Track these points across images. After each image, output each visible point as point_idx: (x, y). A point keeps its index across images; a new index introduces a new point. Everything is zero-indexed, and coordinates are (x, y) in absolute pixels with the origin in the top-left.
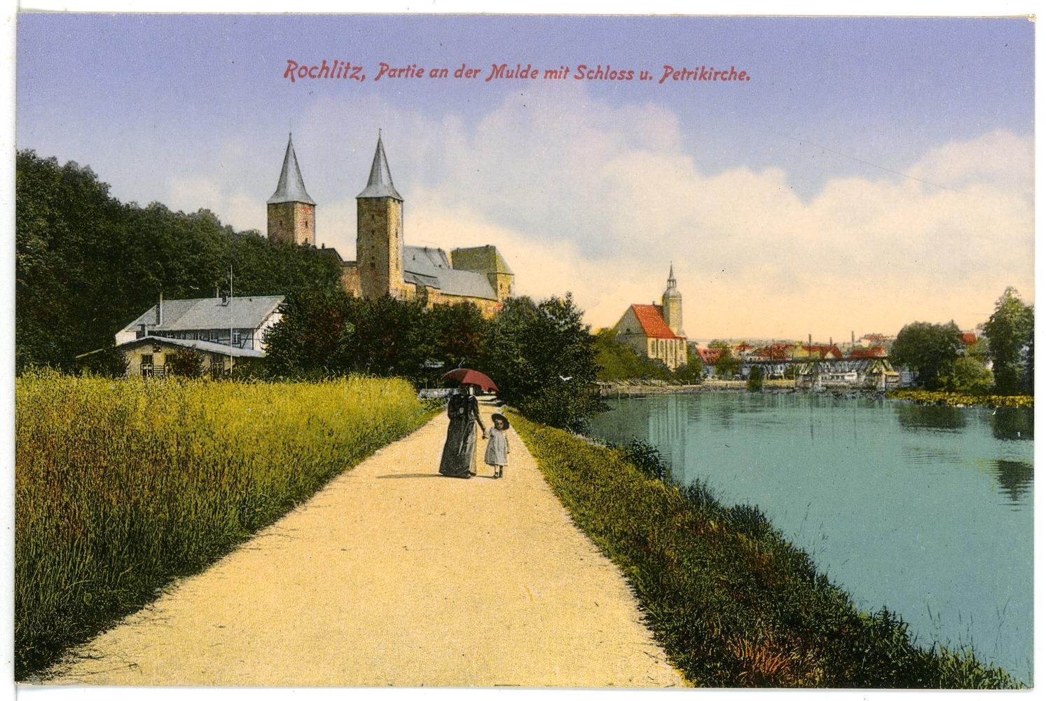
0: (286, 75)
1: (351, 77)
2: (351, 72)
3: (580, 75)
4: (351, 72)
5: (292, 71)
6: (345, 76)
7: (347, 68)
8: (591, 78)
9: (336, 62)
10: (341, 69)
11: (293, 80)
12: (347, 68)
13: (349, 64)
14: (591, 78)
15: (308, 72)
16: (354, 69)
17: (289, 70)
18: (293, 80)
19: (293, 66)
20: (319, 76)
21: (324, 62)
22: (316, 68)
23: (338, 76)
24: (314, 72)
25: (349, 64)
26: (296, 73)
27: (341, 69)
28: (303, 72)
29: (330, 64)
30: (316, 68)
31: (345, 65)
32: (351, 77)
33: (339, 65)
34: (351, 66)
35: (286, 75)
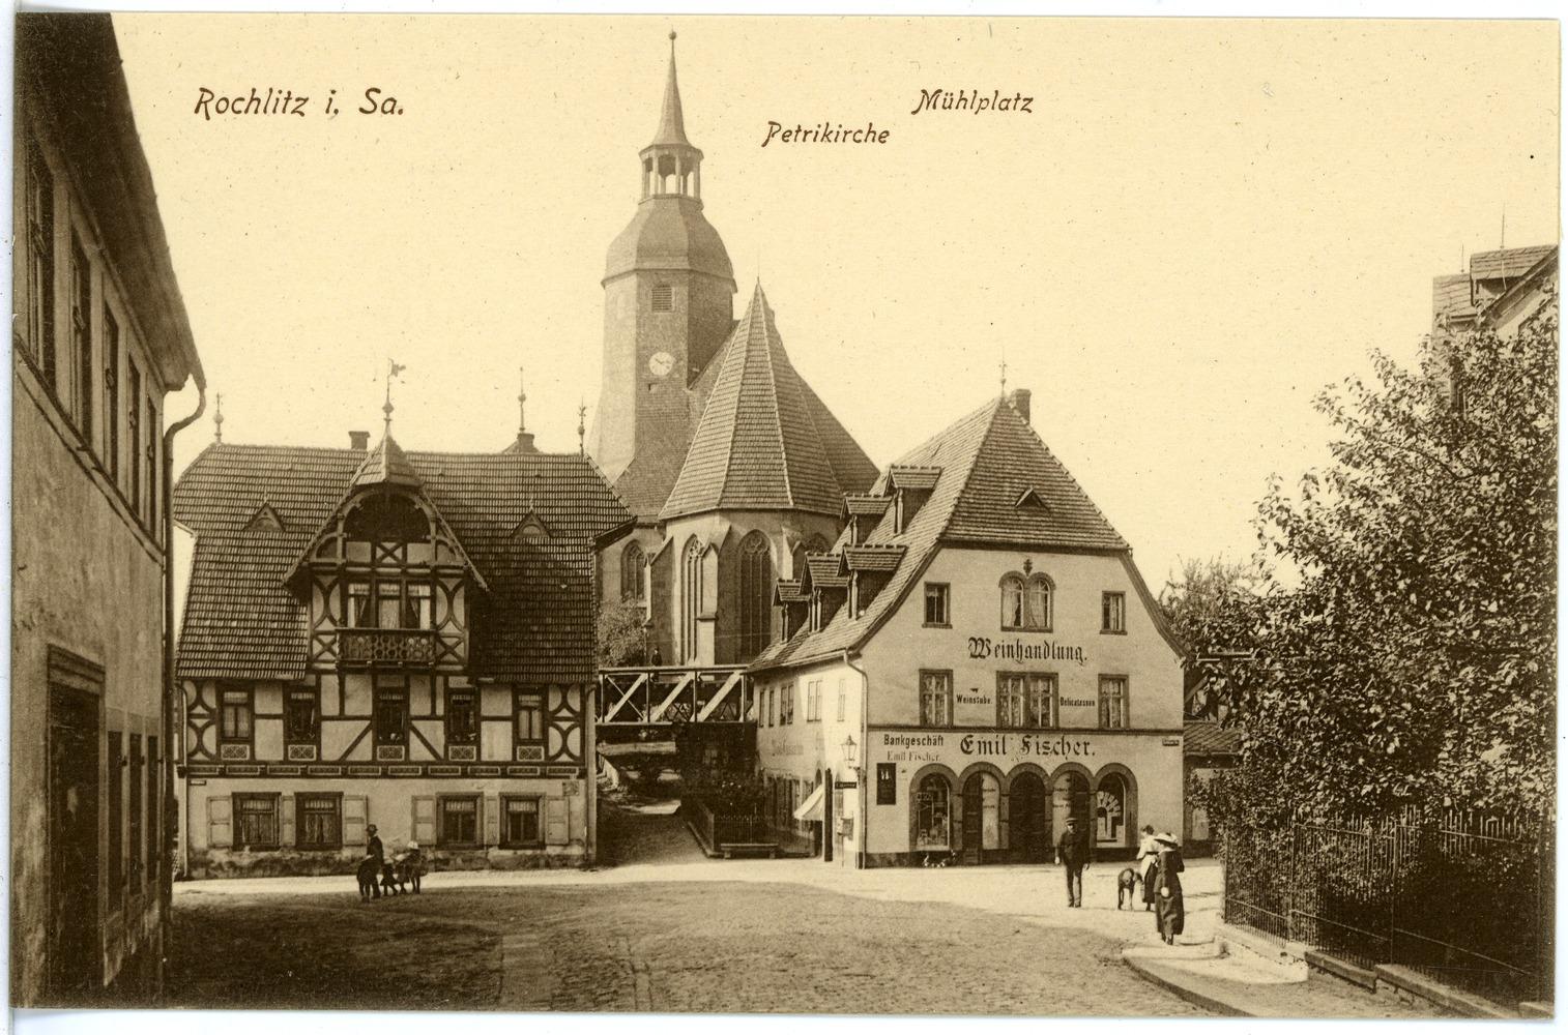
0: (197, 111)
1: (293, 112)
2: (292, 104)
3: (370, 107)
4: (292, 104)
6: (284, 111)
7: (288, 99)
8: (239, 112)
9: (271, 90)
11: (208, 118)
12: (288, 99)
13: (289, 93)
14: (239, 112)
15: (228, 105)
16: (298, 100)
17: (200, 102)
18: (208, 118)
19: (207, 96)
20: (246, 111)
22: (242, 99)
23: (274, 111)
24: (240, 106)
25: (289, 93)
26: (211, 106)
28: (222, 106)
29: (262, 94)
30: (242, 99)
32: (293, 112)
33: (275, 94)
34: (294, 96)
35: (197, 111)
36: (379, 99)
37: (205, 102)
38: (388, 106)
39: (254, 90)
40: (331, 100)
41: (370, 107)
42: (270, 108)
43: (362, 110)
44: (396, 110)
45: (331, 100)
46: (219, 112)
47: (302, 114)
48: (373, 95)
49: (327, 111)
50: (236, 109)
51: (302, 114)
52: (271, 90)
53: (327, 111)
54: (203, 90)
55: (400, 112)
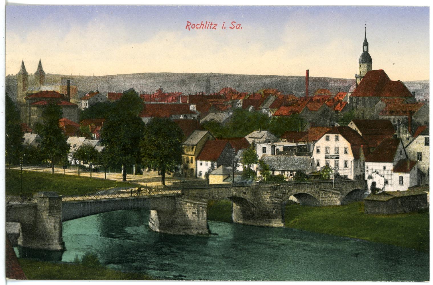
0: (186, 28)
1: (213, 28)
2: (213, 26)
3: (233, 27)
4: (213, 26)
5: (189, 26)
6: (210, 28)
7: (212, 24)
9: (207, 22)
10: (209, 25)
11: (189, 30)
12: (212, 24)
13: (212, 23)
14: (197, 28)
16: (214, 25)
18: (189, 30)
19: (189, 24)
20: (200, 28)
21: (202, 22)
22: (199, 25)
23: (208, 28)
24: (198, 26)
25: (212, 23)
26: (190, 26)
27: (209, 25)
28: (193, 26)
29: (204, 23)
30: (199, 25)
31: (211, 23)
32: (213, 28)
33: (208, 23)
34: (213, 24)
35: (186, 28)
36: (235, 25)
37: (189, 26)
38: (238, 27)
39: (202, 22)
40: (223, 25)
41: (233, 27)
42: (206, 27)
43: (230, 28)
44: (240, 27)
45: (223, 25)
46: (192, 28)
47: (215, 29)
48: (233, 23)
49: (223, 28)
50: (197, 27)
51: (215, 29)
52: (207, 22)
53: (223, 28)
54: (188, 22)
55: (241, 28)
